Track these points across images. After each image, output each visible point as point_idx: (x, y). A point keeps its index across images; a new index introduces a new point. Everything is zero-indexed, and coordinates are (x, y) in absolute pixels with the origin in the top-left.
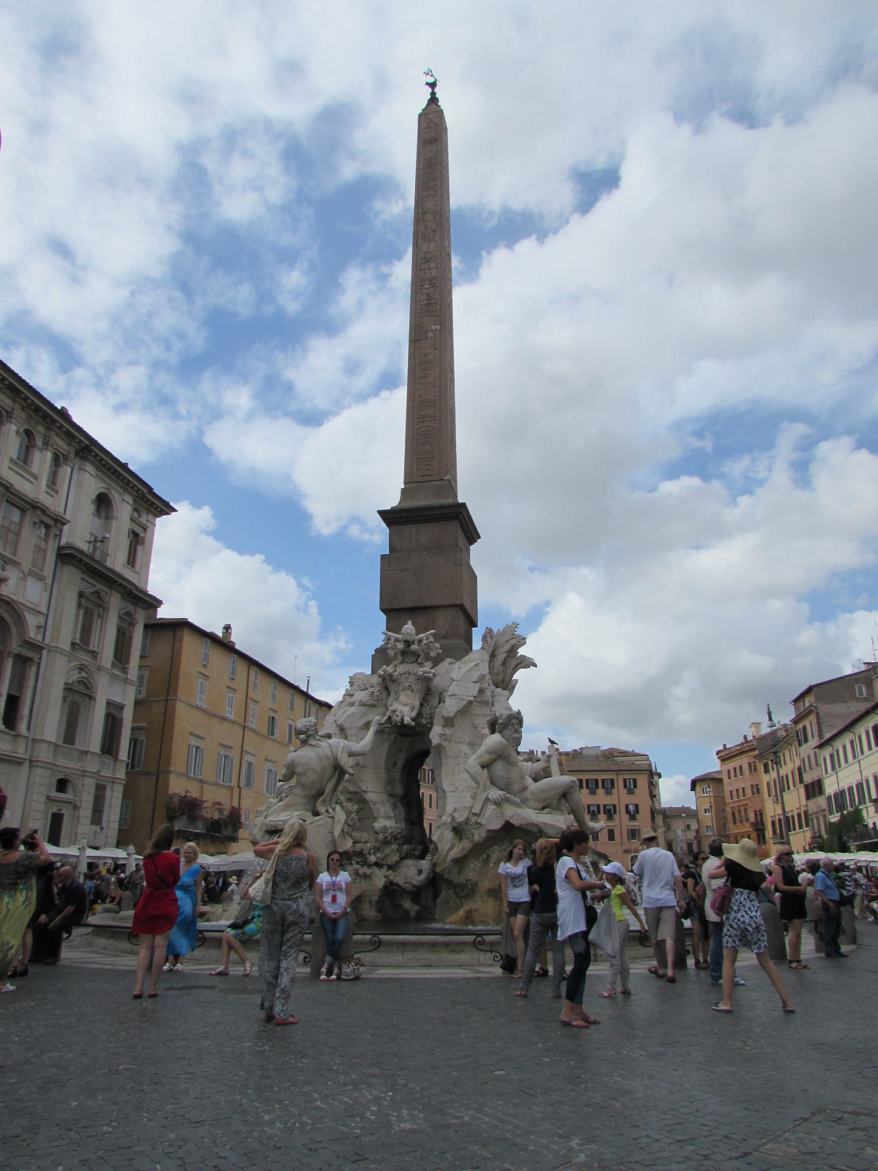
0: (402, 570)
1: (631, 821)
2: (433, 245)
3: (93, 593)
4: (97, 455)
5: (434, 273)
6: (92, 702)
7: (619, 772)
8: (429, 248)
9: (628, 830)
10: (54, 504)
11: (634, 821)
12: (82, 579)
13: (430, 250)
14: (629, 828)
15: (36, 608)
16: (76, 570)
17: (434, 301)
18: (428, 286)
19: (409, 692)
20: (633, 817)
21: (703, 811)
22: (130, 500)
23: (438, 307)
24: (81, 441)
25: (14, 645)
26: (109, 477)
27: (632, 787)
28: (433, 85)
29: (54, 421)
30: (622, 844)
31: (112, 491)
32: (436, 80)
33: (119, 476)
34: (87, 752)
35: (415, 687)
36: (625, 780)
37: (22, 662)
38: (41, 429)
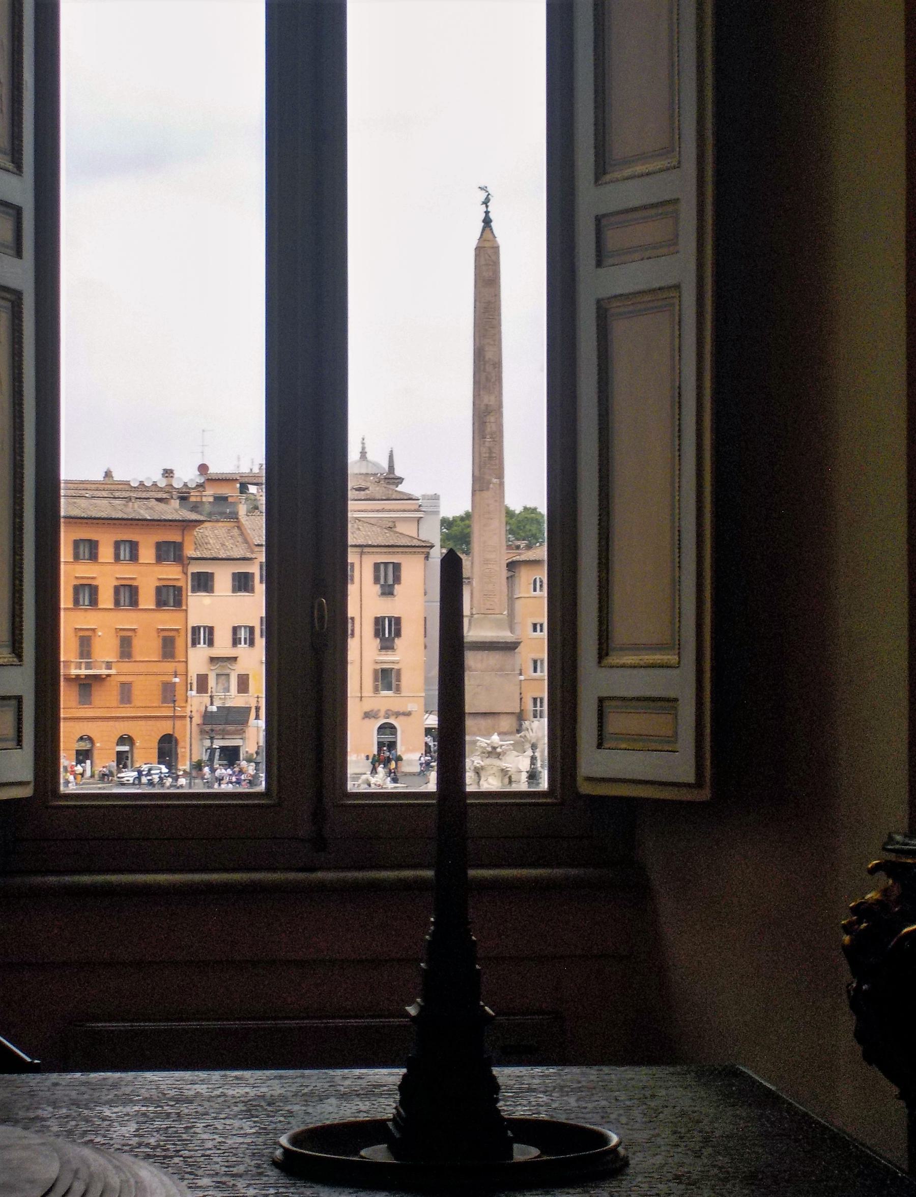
0: (479, 686)
1: (383, 652)
2: (493, 398)
5: (494, 428)
7: (366, 550)
8: (489, 401)
9: (376, 671)
11: (390, 653)
13: (491, 403)
14: (379, 667)
17: (494, 455)
18: (490, 440)
19: (493, 777)
20: (387, 645)
21: (531, 628)
23: (497, 462)
27: (390, 582)
28: (486, 202)
30: (361, 700)
32: (489, 194)
35: (497, 774)
36: (377, 566)
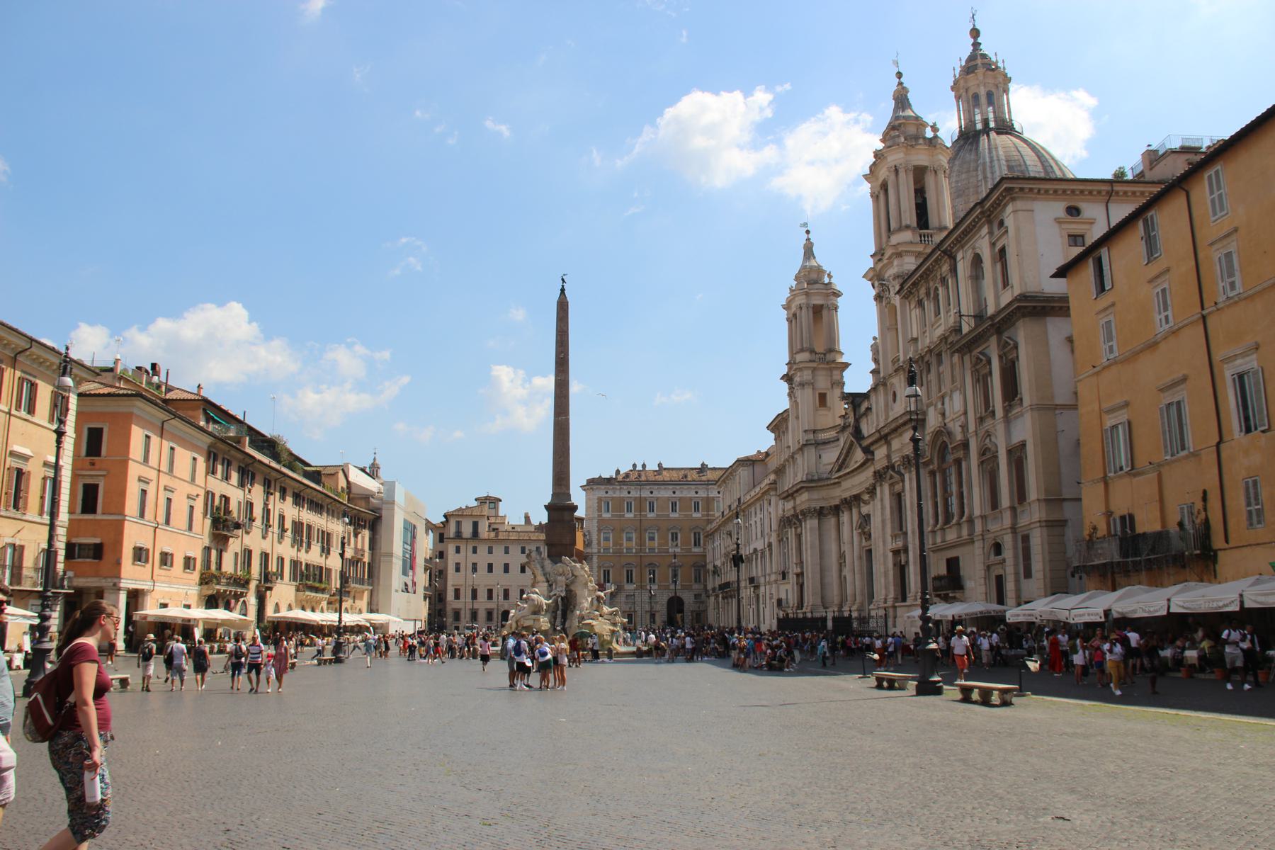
29: (929, 266)
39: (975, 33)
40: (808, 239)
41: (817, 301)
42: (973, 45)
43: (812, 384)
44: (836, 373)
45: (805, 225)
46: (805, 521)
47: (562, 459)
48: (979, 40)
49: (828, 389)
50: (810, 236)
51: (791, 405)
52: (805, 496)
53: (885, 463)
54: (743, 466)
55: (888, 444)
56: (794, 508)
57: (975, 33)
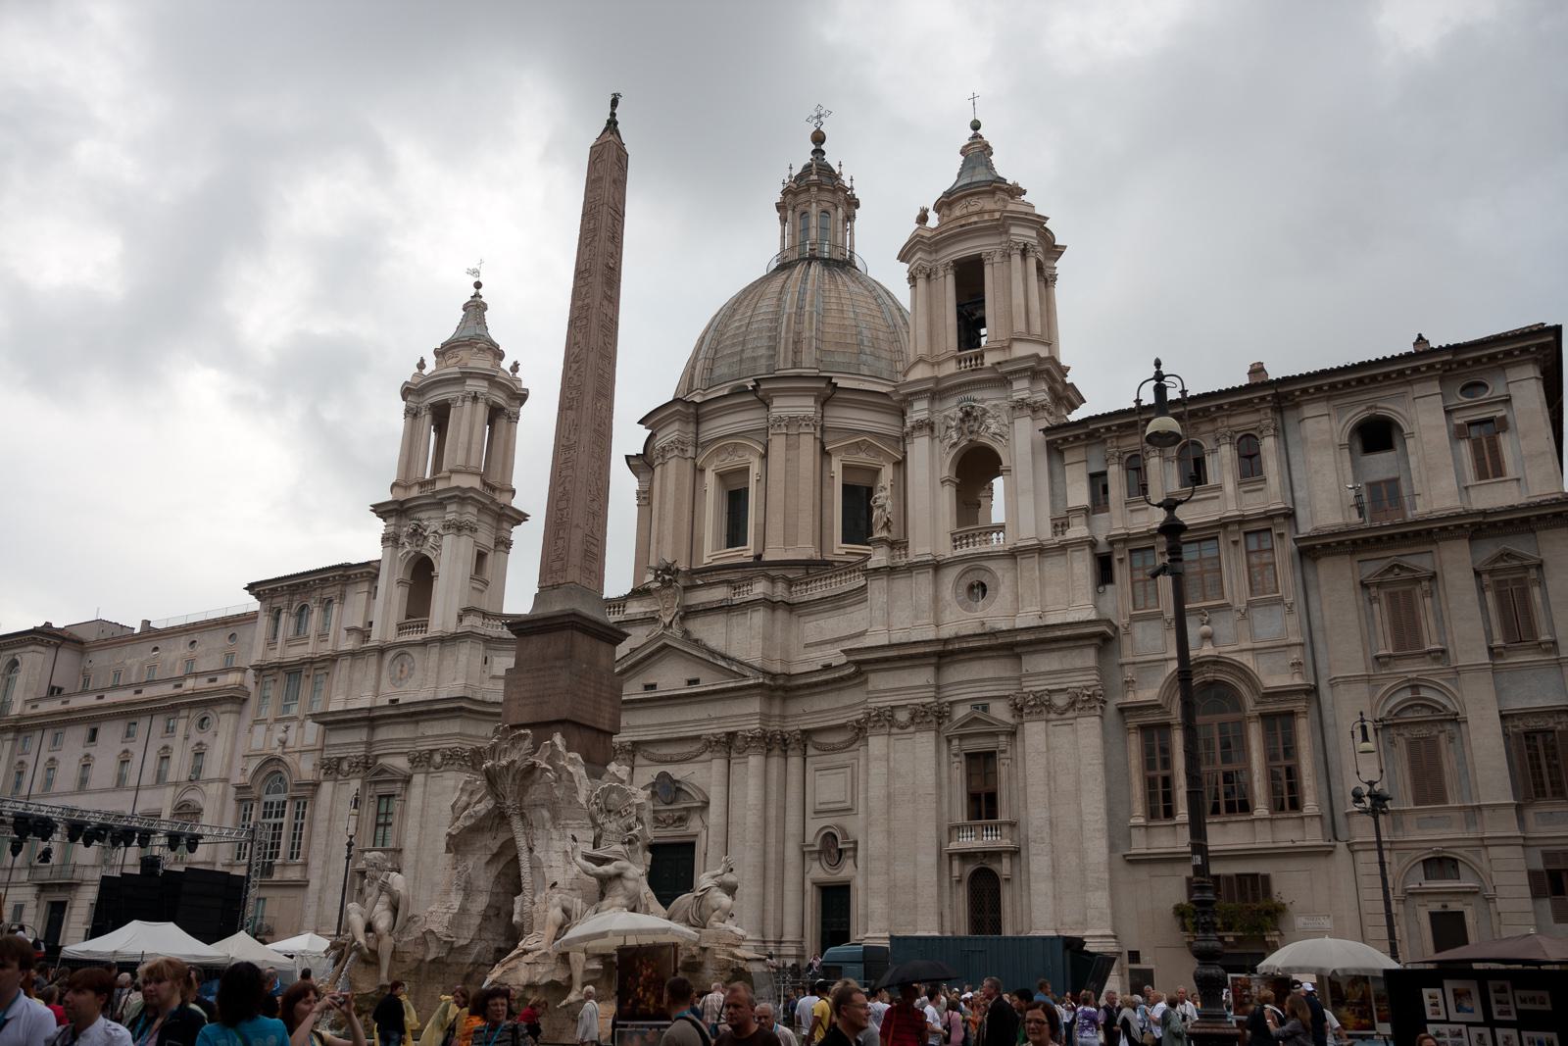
3: (1391, 569)
4: (1305, 391)
6: (1463, 726)
10: (1269, 497)
12: (1359, 561)
15: (1284, 643)
16: (1334, 558)
22: (1435, 387)
24: (1263, 399)
25: (1250, 705)
26: (1362, 392)
29: (1208, 409)
31: (1379, 405)
33: (1373, 379)
34: (1479, 807)
37: (1279, 724)
38: (1205, 427)
39: (819, 138)
40: (477, 295)
41: (500, 398)
42: (814, 152)
43: (476, 530)
44: (505, 525)
45: (476, 272)
46: (427, 773)
47: (596, 506)
48: (823, 147)
49: (490, 549)
50: (481, 291)
51: (393, 557)
52: (453, 726)
53: (928, 698)
54: (41, 643)
55: (938, 668)
56: (369, 744)
57: (819, 138)
